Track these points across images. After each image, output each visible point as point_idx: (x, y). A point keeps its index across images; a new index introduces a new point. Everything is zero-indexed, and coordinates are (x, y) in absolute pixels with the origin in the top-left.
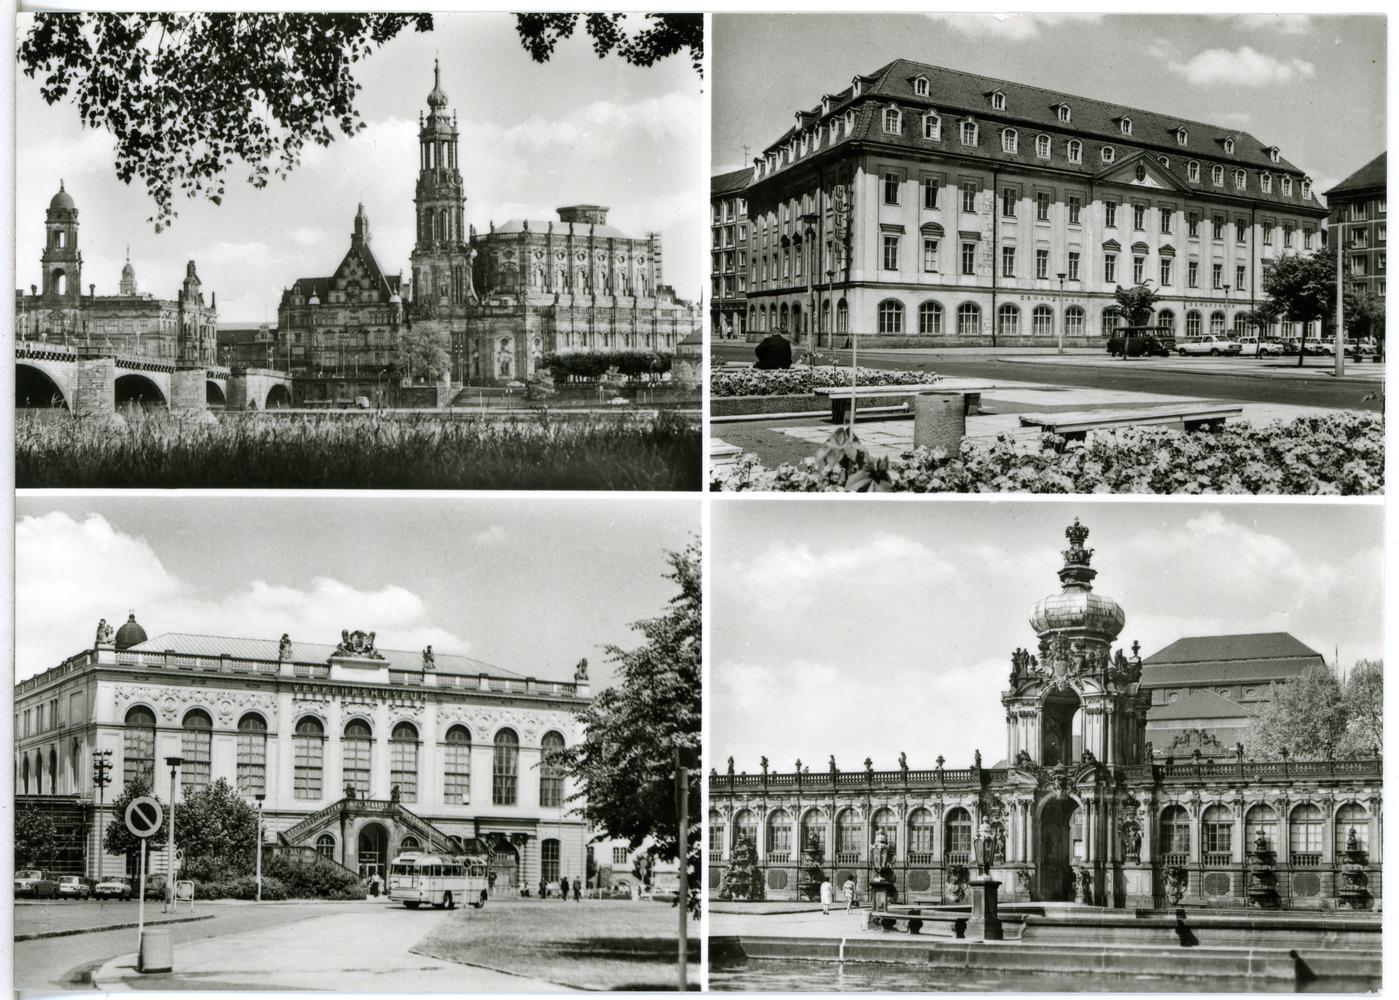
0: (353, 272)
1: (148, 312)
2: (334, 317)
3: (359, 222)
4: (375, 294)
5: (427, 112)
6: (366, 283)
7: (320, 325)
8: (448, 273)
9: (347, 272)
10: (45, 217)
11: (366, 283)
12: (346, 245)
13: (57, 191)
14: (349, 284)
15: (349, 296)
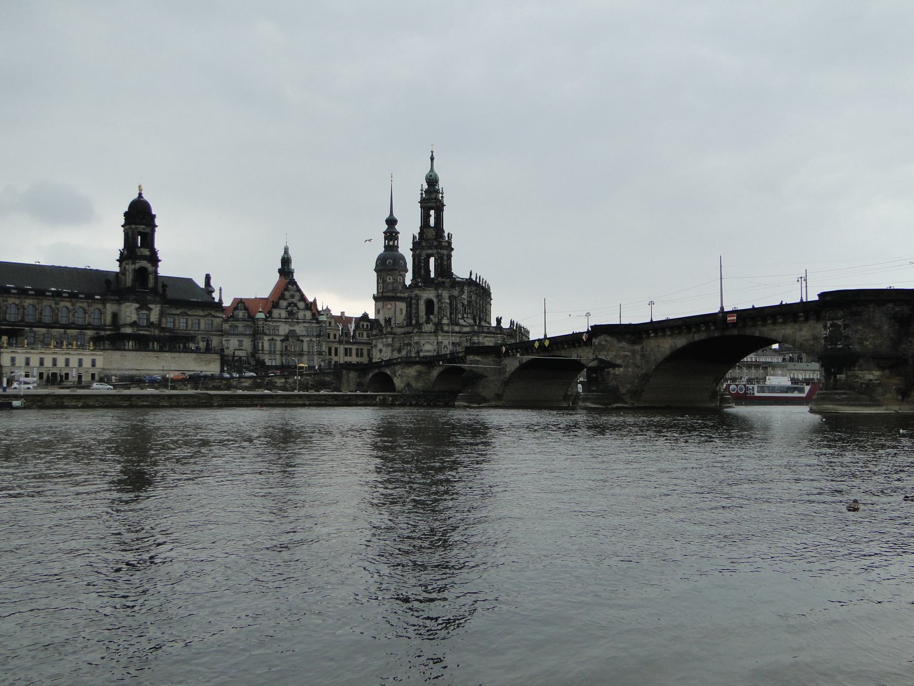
0: (293, 296)
1: (213, 313)
2: (276, 328)
3: (286, 261)
4: (308, 314)
5: (426, 186)
6: (301, 305)
7: (266, 334)
8: (448, 301)
9: (287, 294)
10: (122, 221)
11: (301, 305)
12: (276, 277)
13: (136, 196)
14: (289, 304)
15: (291, 314)
